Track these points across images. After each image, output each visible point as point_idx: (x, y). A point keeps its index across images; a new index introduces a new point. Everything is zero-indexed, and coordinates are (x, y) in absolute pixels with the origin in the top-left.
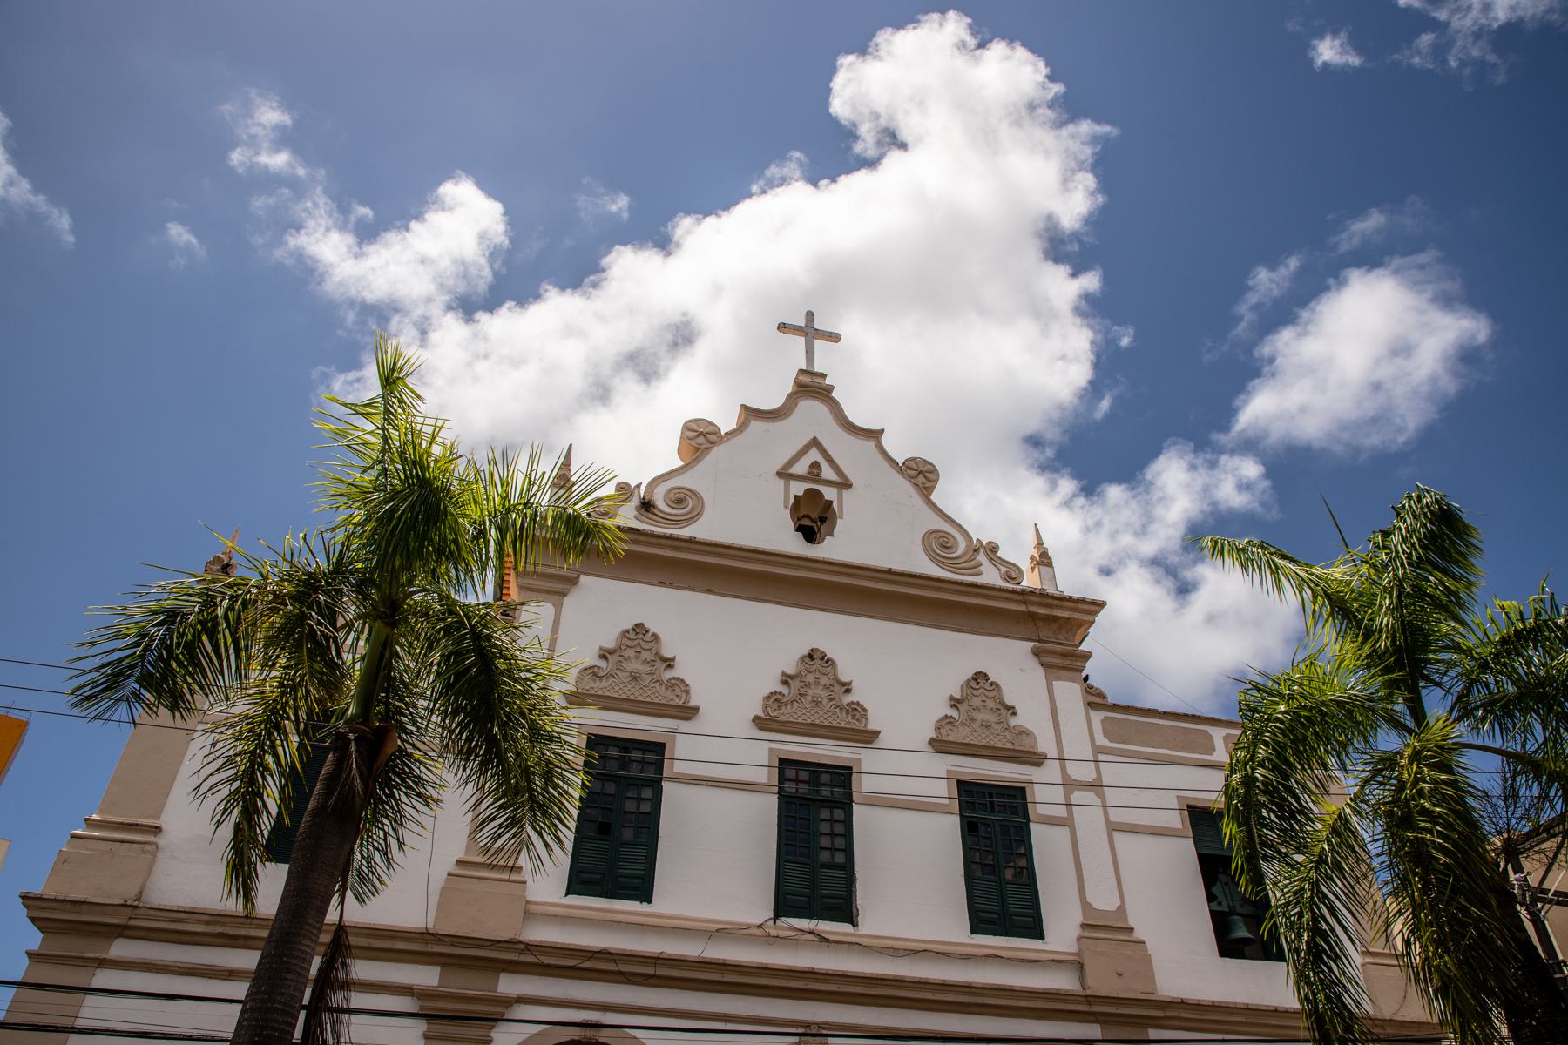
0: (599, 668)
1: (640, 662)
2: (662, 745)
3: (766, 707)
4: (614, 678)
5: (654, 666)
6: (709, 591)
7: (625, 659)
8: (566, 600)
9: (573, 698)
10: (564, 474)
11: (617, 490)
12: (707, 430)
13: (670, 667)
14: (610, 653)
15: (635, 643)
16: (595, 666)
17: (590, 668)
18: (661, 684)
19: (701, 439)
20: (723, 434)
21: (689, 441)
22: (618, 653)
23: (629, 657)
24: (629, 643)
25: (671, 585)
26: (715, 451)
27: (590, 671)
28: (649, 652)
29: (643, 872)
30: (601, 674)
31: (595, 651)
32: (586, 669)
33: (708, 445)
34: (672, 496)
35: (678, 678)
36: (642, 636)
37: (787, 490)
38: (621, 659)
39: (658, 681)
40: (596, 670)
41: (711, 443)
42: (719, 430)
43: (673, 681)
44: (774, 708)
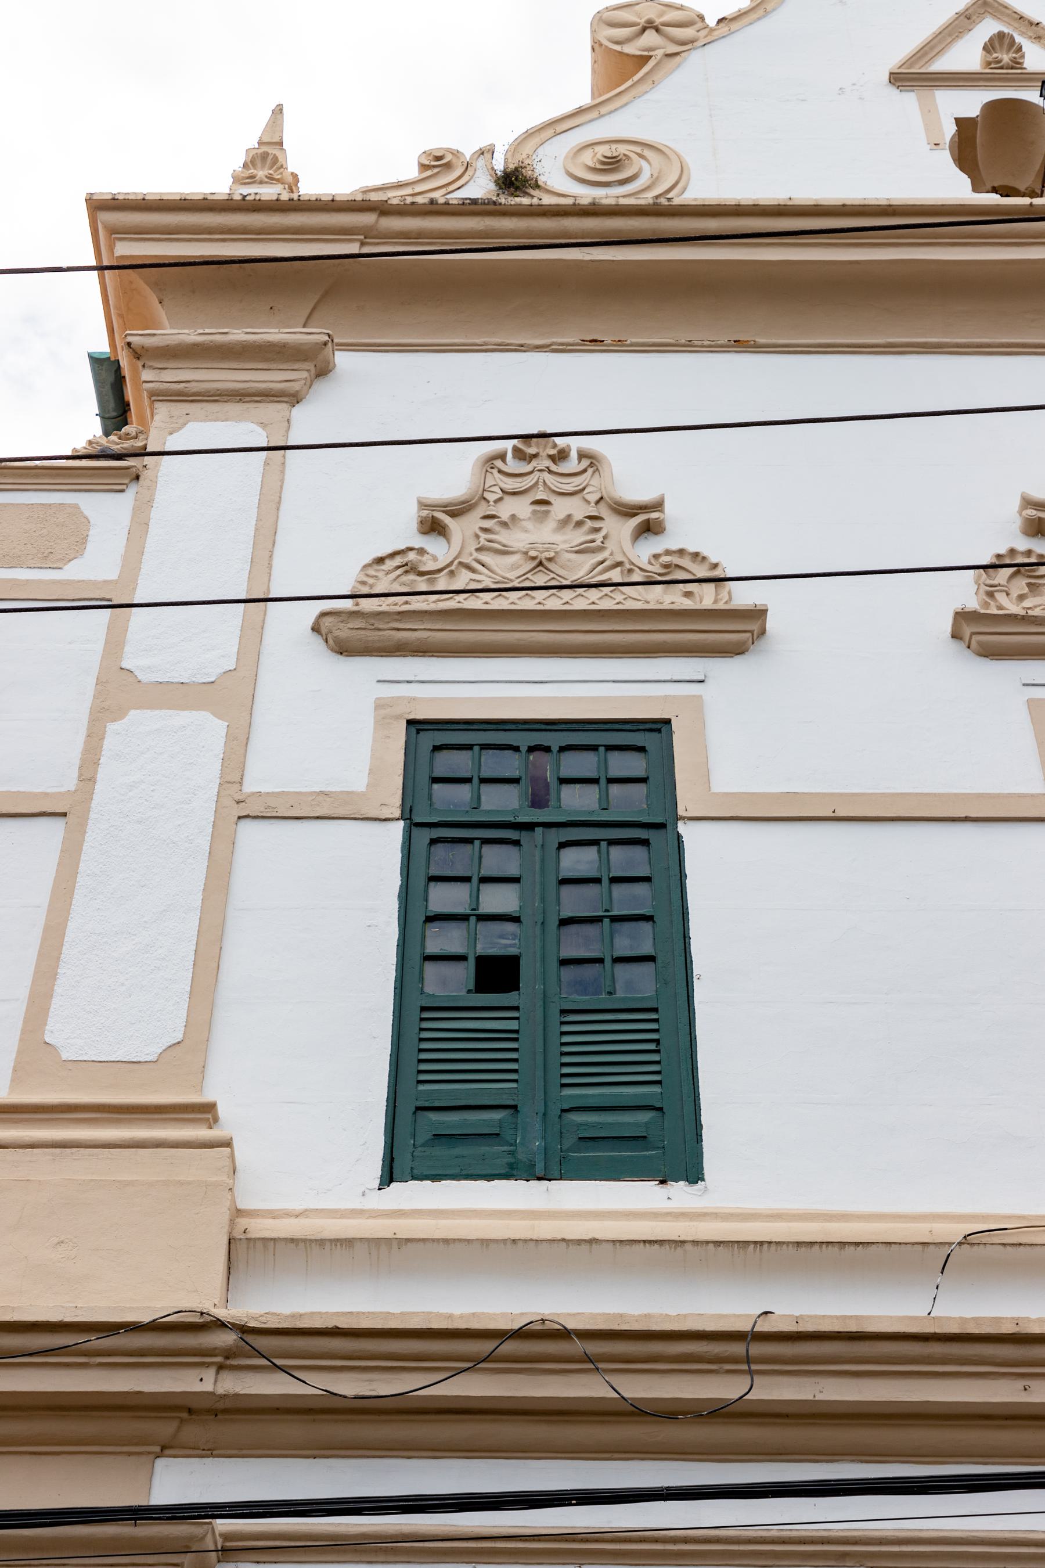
0: (421, 551)
1: (551, 524)
2: (661, 726)
3: (991, 595)
4: (473, 570)
5: (597, 530)
6: (739, 346)
7: (504, 524)
9: (344, 631)
11: (423, 167)
12: (665, 18)
13: (649, 529)
14: (453, 514)
15: (528, 482)
16: (411, 549)
17: (393, 555)
18: (630, 571)
19: (650, 38)
20: (711, 22)
21: (618, 48)
22: (482, 510)
23: (513, 517)
24: (510, 484)
25: (620, 346)
26: (695, 59)
27: (398, 561)
28: (576, 500)
29: (656, 1089)
30: (430, 566)
31: (410, 515)
32: (380, 560)
33: (674, 48)
34: (588, 158)
35: (681, 552)
36: (548, 463)
37: (930, 114)
38: (488, 524)
39: (619, 564)
40: (412, 556)
41: (683, 43)
42: (702, 18)
43: (666, 559)
44: (1015, 593)
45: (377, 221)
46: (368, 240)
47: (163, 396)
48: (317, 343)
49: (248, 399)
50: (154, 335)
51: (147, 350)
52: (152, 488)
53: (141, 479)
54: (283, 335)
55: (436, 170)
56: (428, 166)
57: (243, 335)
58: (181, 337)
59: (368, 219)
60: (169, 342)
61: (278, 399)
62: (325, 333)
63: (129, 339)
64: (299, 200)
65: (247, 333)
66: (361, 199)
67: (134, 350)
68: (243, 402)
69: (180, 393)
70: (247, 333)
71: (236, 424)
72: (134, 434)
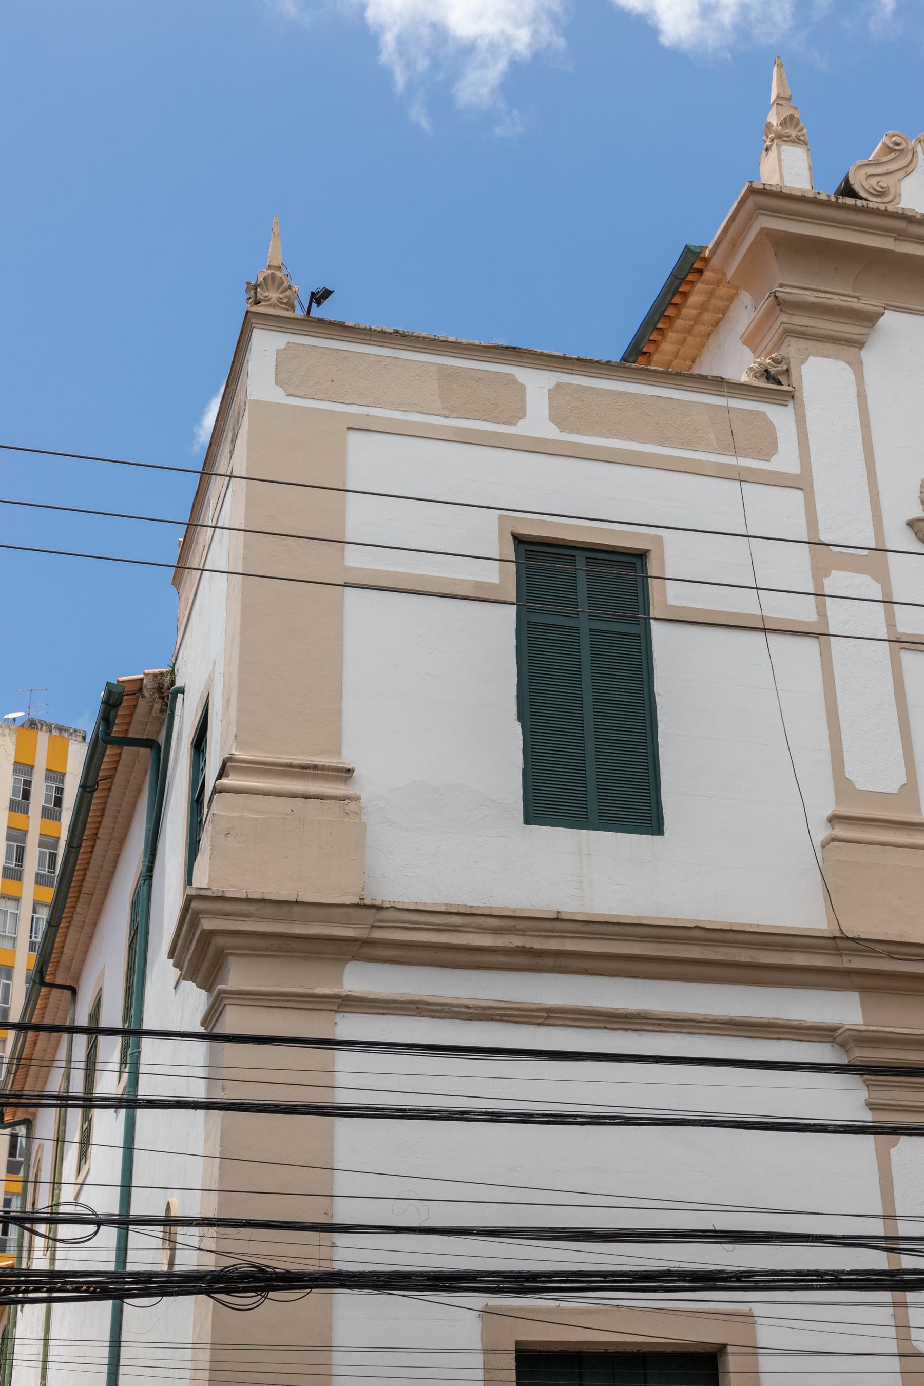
8: (865, 354)
10: (791, 117)
45: (906, 227)
46: (899, 237)
47: (793, 333)
48: (879, 313)
49: (838, 342)
50: (791, 293)
51: (786, 302)
52: (802, 406)
53: (795, 397)
54: (861, 305)
55: (898, 153)
56: (892, 149)
57: (839, 301)
58: (806, 297)
59: (901, 225)
60: (798, 300)
61: (854, 345)
62: (883, 307)
63: (778, 294)
64: (867, 207)
65: (841, 300)
66: (901, 212)
67: (778, 300)
68: (836, 344)
69: (802, 333)
70: (841, 300)
71: (835, 361)
72: (780, 360)
